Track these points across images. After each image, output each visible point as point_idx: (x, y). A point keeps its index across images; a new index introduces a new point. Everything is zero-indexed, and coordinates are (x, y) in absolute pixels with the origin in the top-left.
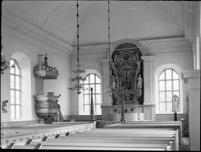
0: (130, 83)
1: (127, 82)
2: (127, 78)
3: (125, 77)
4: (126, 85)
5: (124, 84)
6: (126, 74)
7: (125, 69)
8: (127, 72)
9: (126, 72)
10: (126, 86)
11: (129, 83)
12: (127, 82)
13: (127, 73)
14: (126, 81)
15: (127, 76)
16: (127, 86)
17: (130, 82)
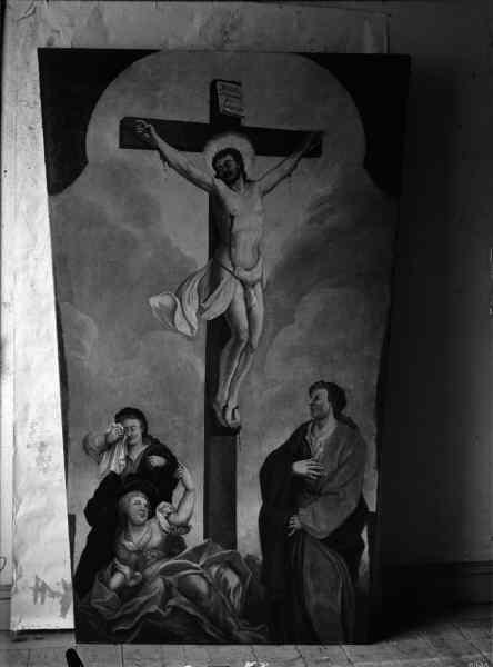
0: (301, 467)
1: (221, 437)
2: (220, 334)
3: (190, 320)
4: (190, 506)
5: (159, 483)
6: (195, 248)
7: (189, 137)
8: (234, 201)
9: (216, 204)
10: (195, 537)
11: (276, 473)
12: (233, 432)
13: (221, 234)
14: (210, 413)
15: (229, 294)
16: (232, 544)
17: (297, 446)
